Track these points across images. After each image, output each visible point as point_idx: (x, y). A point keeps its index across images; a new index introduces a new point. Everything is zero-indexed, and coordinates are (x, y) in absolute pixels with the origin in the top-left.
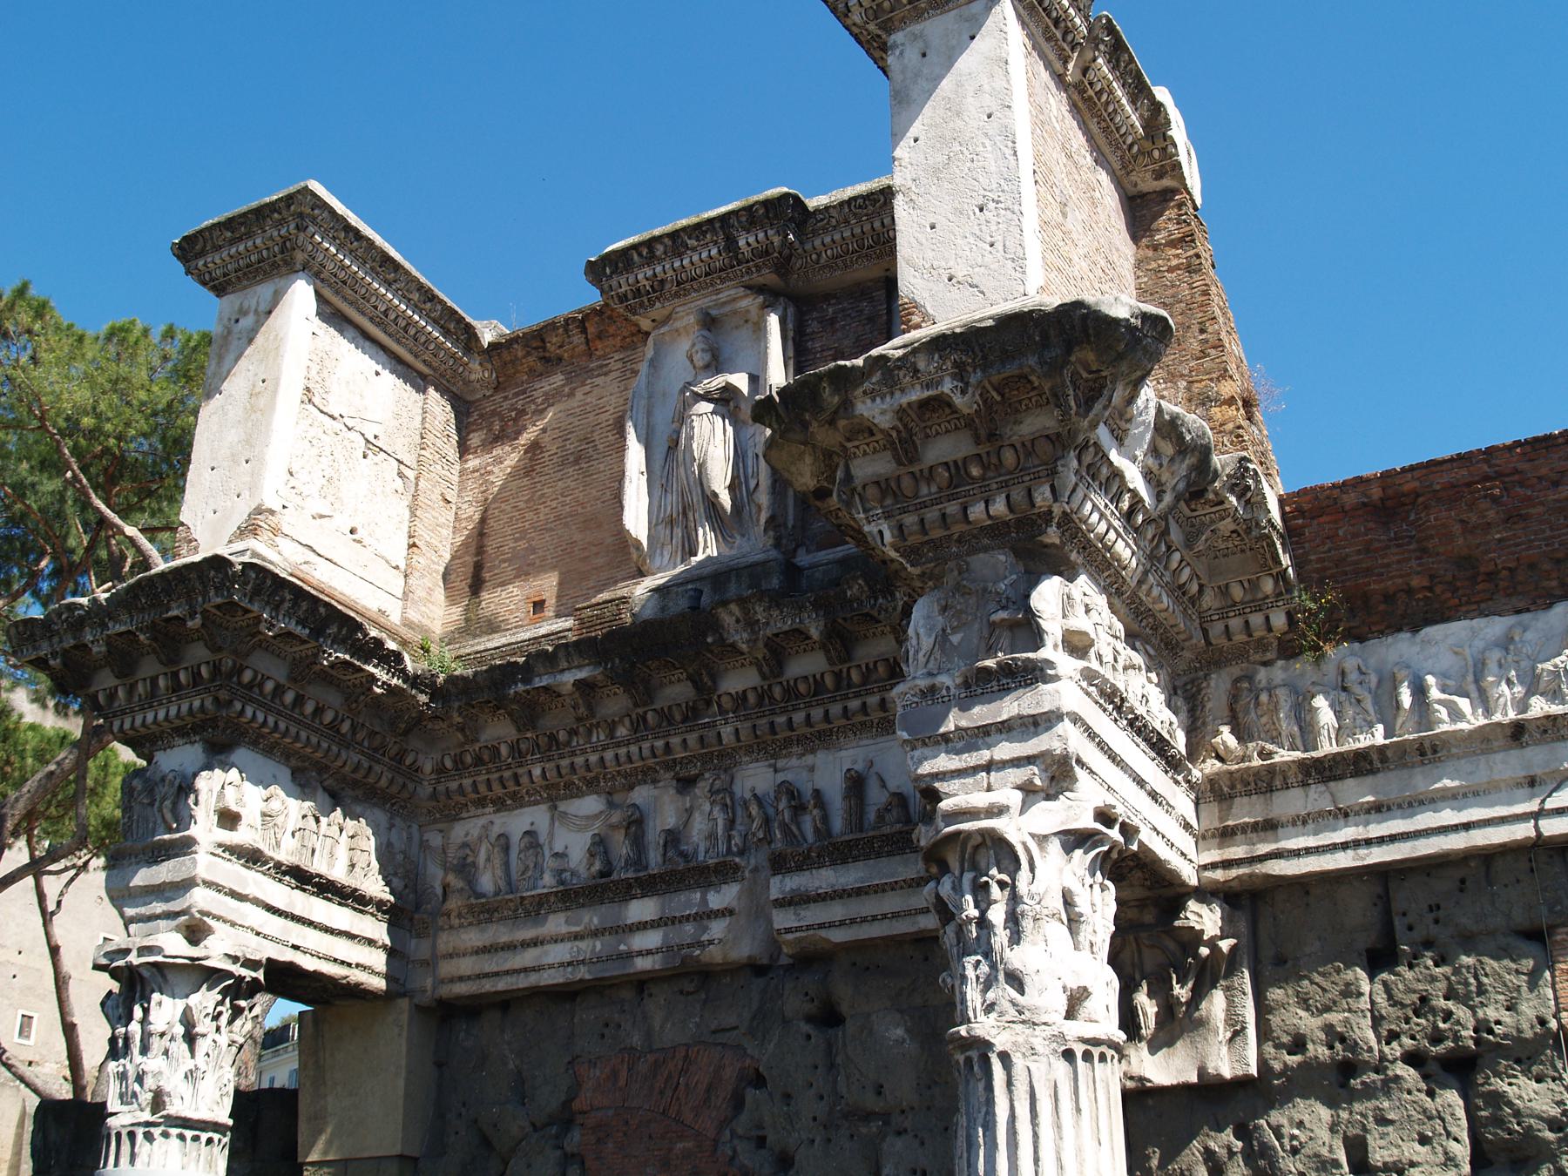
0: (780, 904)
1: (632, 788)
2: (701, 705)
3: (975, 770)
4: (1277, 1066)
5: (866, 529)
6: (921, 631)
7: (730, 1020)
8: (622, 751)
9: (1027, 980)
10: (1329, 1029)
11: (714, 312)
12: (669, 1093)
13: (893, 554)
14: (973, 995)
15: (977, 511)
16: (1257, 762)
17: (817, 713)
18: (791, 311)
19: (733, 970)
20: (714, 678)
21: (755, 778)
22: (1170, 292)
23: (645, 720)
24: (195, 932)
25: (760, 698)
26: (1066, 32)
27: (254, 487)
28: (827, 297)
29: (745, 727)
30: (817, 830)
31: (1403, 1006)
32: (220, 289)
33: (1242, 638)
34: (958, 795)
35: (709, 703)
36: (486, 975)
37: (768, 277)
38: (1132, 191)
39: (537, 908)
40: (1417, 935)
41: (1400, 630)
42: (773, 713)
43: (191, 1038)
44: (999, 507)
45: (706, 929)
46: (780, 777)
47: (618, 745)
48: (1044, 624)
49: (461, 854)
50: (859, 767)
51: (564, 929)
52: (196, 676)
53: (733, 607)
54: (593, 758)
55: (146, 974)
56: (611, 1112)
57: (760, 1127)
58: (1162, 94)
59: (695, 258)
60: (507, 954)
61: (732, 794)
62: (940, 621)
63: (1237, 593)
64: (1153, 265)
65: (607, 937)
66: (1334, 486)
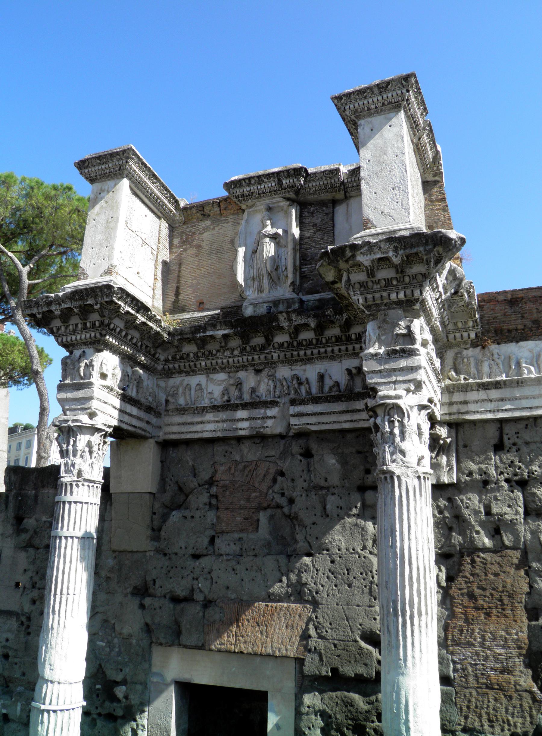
0: (293, 416)
1: (237, 371)
2: (266, 346)
3: (390, 383)
4: (463, 480)
5: (353, 298)
6: (372, 334)
7: (273, 453)
8: (236, 359)
9: (407, 453)
10: (480, 469)
11: (271, 206)
12: (249, 476)
13: (362, 307)
14: (388, 456)
15: (393, 296)
16: (463, 381)
17: (309, 352)
18: (298, 208)
19: (273, 436)
20: (272, 337)
21: (284, 372)
22: (437, 217)
23: (245, 348)
24: (92, 415)
25: (289, 345)
26: (417, 126)
27: (110, 257)
28: (311, 204)
29: (282, 355)
30: (307, 392)
31: (505, 463)
32: (92, 180)
33: (460, 340)
34: (383, 392)
35: (269, 345)
36: (183, 433)
37: (292, 195)
38: (425, 180)
39: (203, 410)
40: (511, 441)
41: (512, 342)
42: (292, 350)
43: (91, 452)
44: (401, 295)
45: (265, 422)
46: (293, 373)
47: (235, 357)
48: (416, 337)
49: (173, 390)
50: (322, 371)
51: (212, 419)
52: (94, 325)
53: (284, 314)
54: (225, 361)
55: (75, 429)
56: (228, 482)
57: (283, 489)
58: (439, 148)
59: (266, 186)
60: (191, 426)
61: (275, 377)
62: (378, 331)
63: (460, 325)
64: (431, 207)
65: (228, 423)
66: (496, 293)
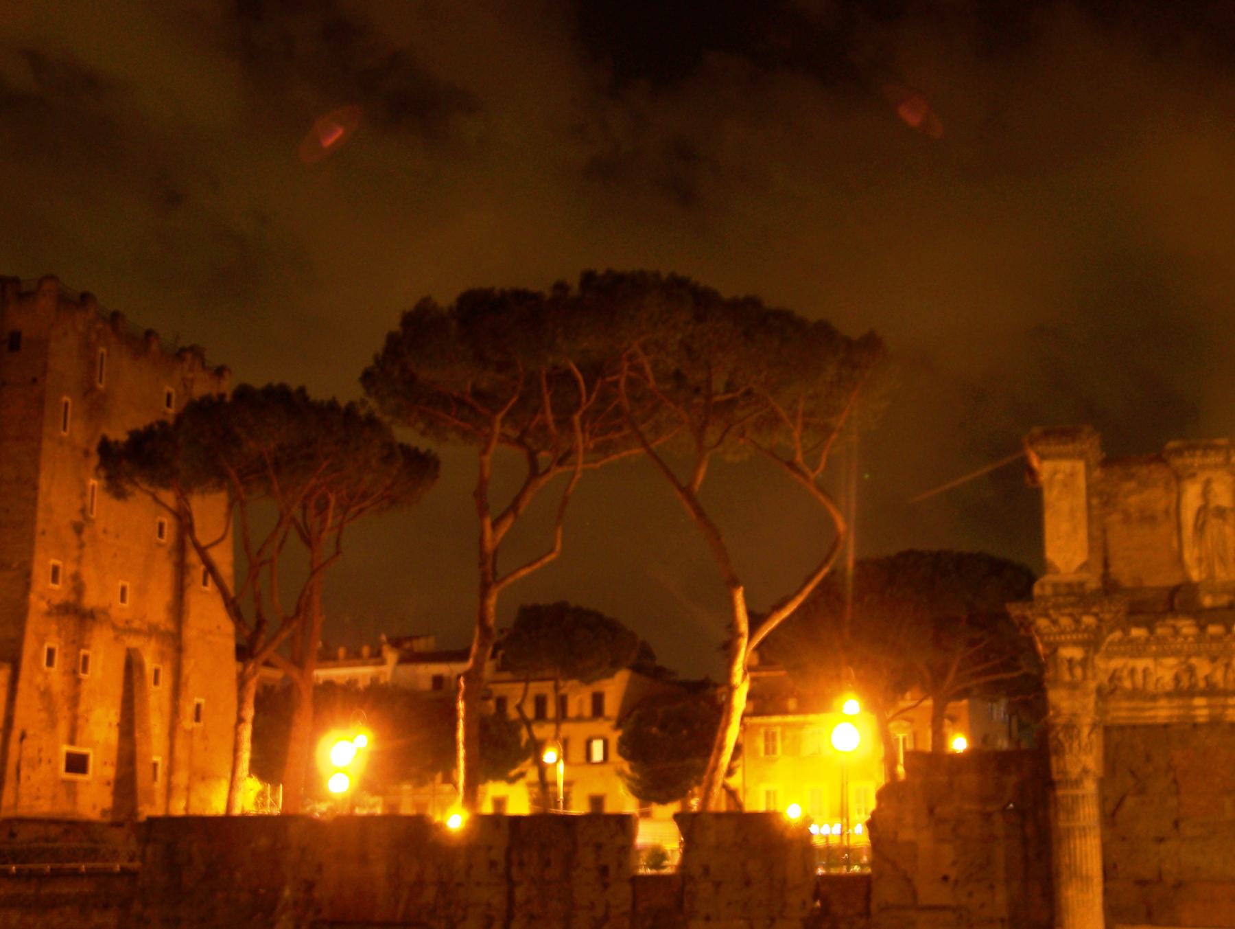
39: (1154, 697)
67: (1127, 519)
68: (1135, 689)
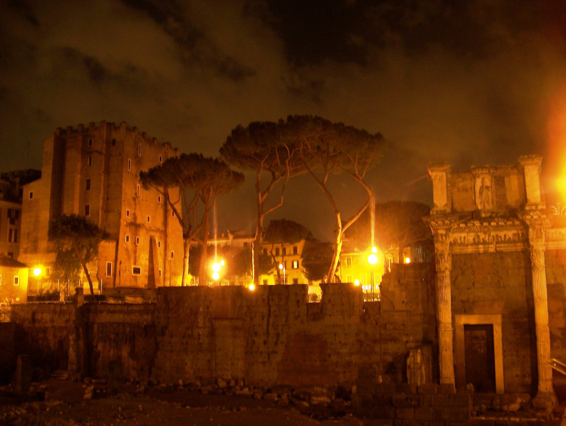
21: (493, 233)
39: (467, 245)
67: (459, 189)
68: (461, 243)
